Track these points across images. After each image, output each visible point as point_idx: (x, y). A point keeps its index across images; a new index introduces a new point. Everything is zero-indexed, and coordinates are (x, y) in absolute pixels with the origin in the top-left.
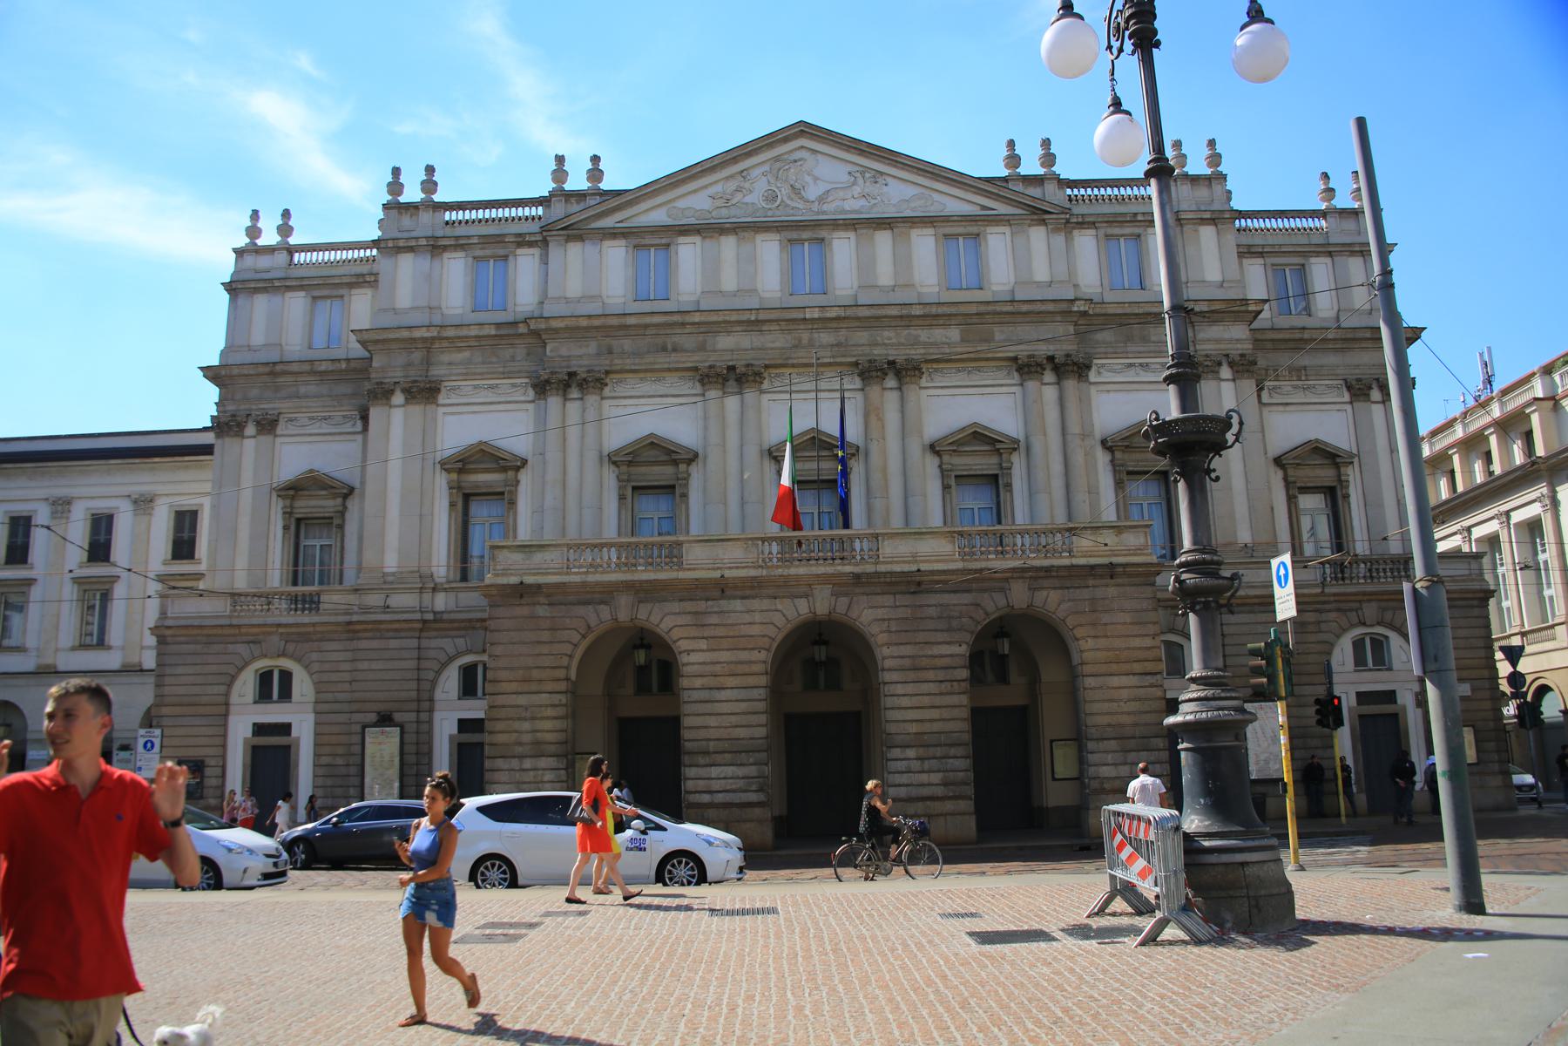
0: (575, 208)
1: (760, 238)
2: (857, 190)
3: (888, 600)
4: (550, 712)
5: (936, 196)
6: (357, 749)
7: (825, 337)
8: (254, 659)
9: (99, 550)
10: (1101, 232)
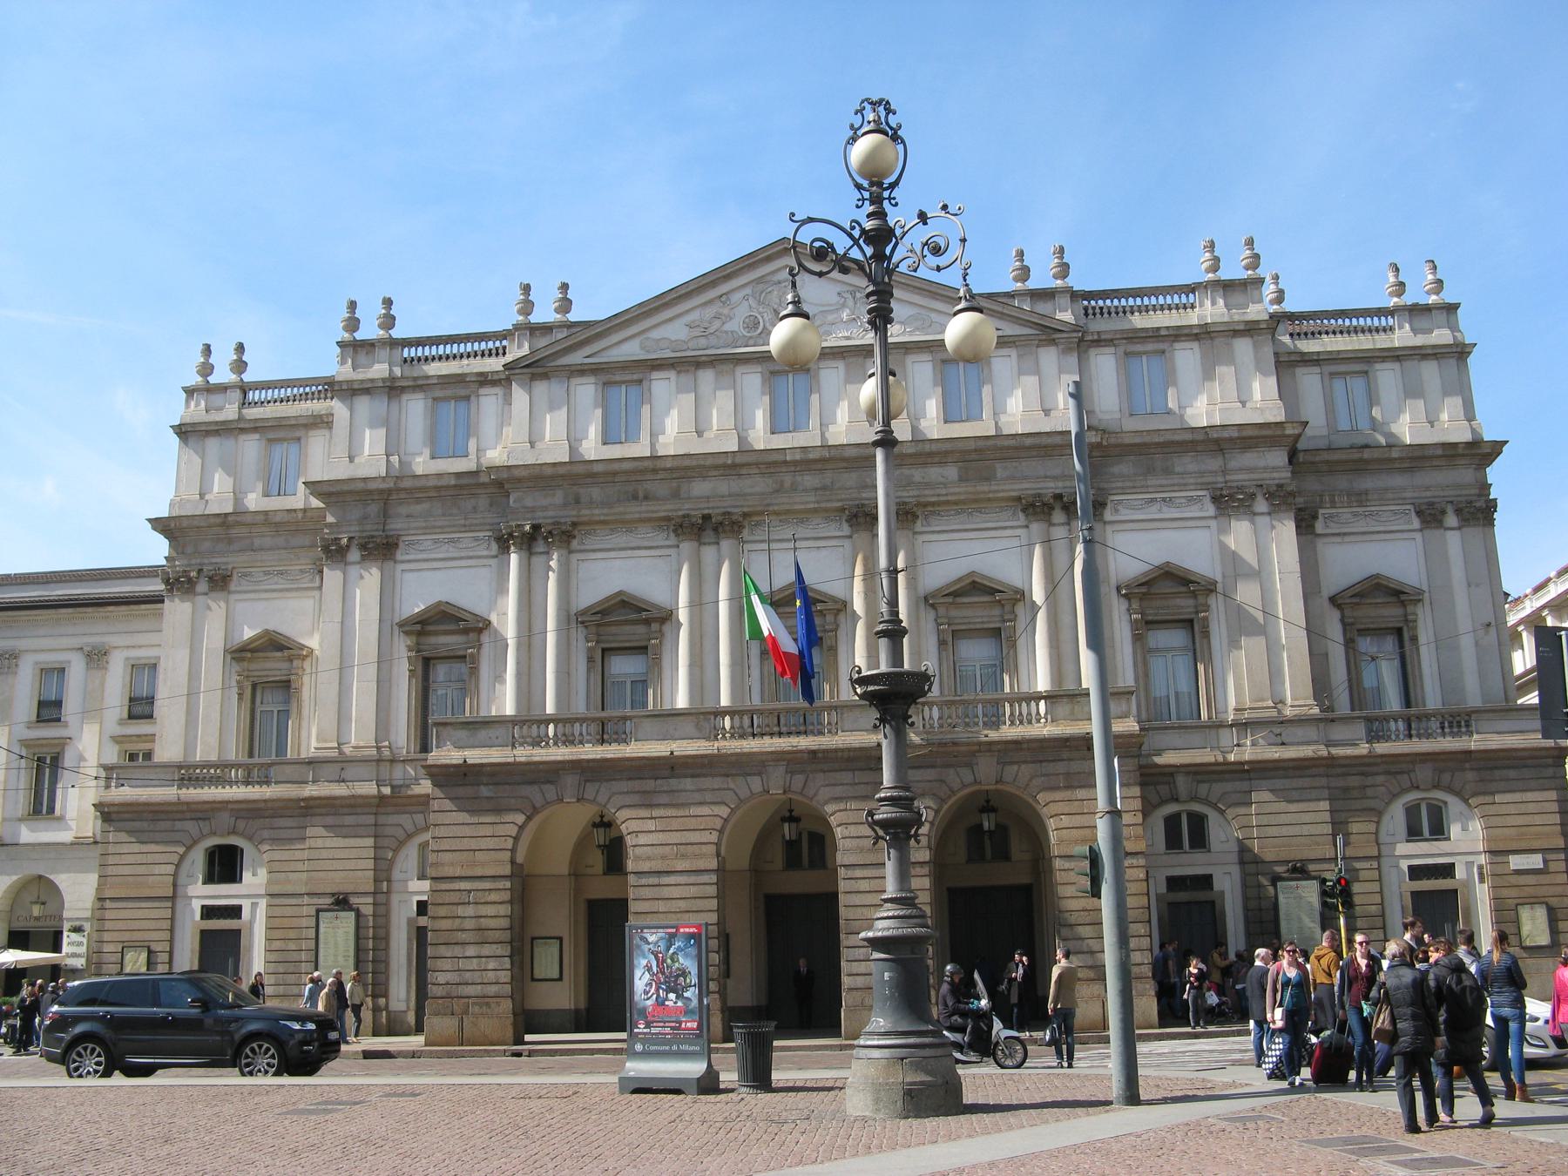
0: (542, 342)
1: (740, 370)
3: (846, 777)
4: (493, 897)
5: (933, 316)
6: (312, 933)
7: (810, 480)
8: (203, 837)
9: (49, 710)
10: (1121, 350)
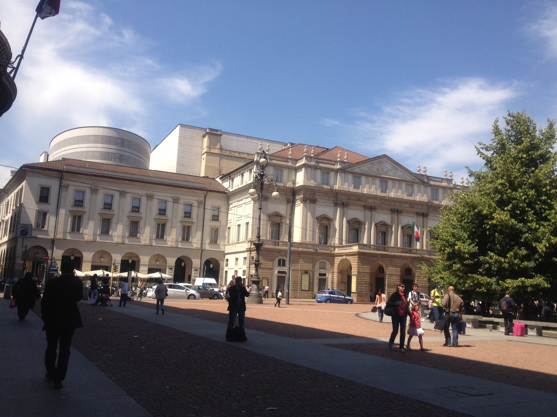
0: (343, 165)
2: (392, 172)
7: (387, 203)
